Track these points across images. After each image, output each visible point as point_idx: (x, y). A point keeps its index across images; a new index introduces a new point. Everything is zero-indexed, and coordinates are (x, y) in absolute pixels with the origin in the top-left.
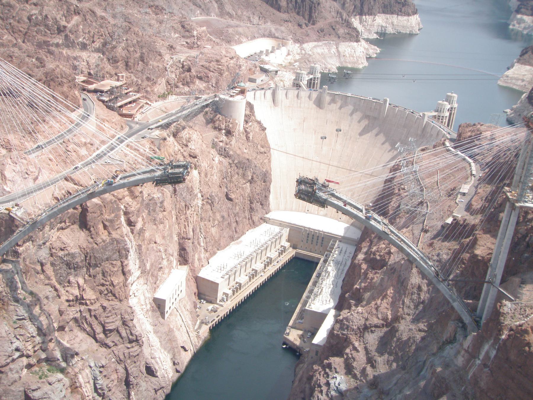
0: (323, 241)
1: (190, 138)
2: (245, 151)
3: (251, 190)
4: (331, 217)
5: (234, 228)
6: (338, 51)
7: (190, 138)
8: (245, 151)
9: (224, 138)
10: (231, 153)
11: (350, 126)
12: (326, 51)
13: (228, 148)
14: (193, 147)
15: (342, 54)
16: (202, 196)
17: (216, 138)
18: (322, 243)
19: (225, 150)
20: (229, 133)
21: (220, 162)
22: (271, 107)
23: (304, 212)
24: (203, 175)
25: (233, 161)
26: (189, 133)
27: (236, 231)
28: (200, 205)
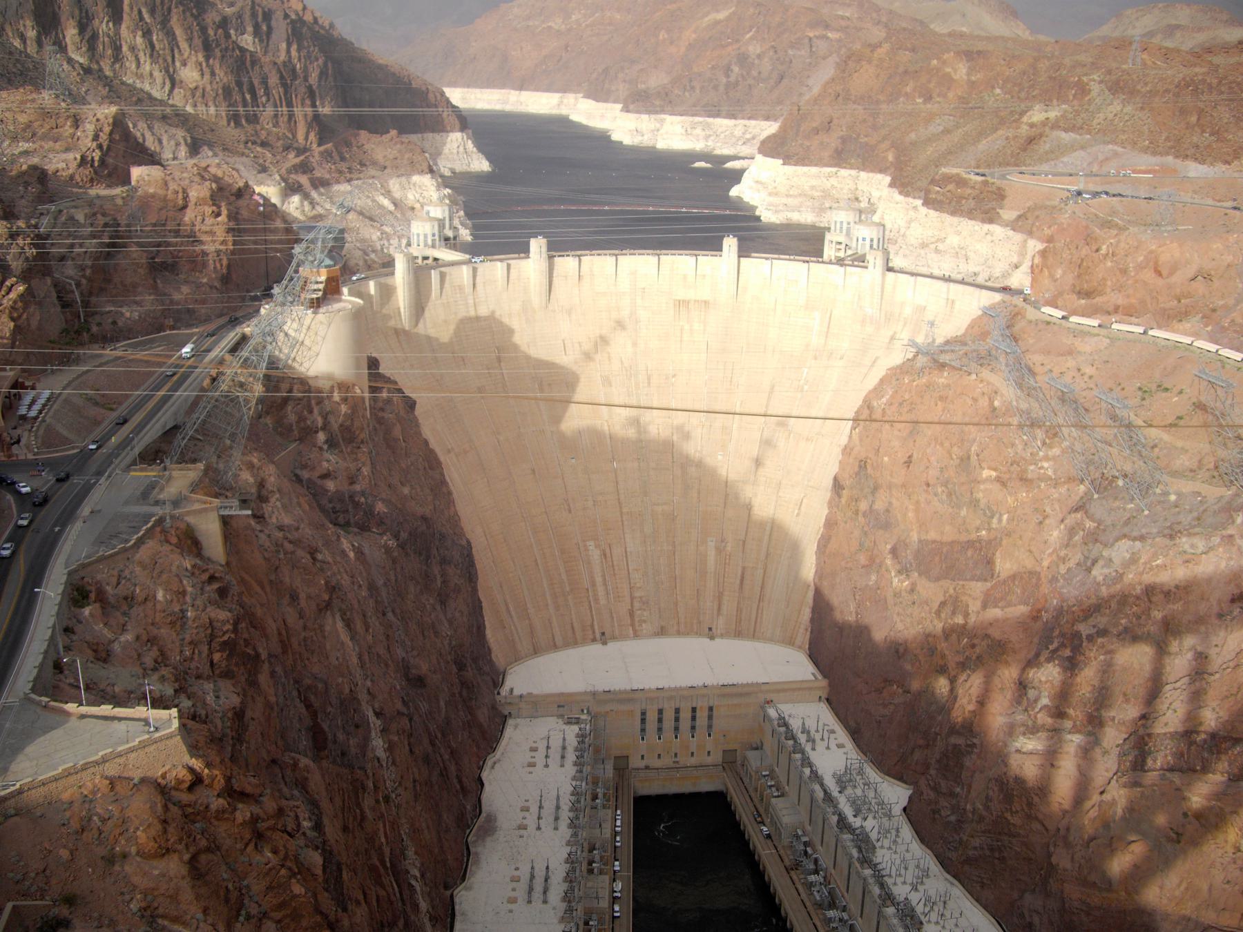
0: (710, 717)
1: (261, 484)
2: (406, 491)
3: (450, 622)
5: (455, 781)
7: (261, 484)
8: (406, 491)
10: (380, 507)
11: (635, 344)
13: (363, 493)
14: (287, 520)
16: (378, 714)
17: (304, 467)
18: (710, 727)
19: (357, 505)
21: (359, 552)
23: (594, 640)
24: (359, 626)
25: (396, 537)
26: (251, 466)
27: (462, 788)
28: (381, 753)
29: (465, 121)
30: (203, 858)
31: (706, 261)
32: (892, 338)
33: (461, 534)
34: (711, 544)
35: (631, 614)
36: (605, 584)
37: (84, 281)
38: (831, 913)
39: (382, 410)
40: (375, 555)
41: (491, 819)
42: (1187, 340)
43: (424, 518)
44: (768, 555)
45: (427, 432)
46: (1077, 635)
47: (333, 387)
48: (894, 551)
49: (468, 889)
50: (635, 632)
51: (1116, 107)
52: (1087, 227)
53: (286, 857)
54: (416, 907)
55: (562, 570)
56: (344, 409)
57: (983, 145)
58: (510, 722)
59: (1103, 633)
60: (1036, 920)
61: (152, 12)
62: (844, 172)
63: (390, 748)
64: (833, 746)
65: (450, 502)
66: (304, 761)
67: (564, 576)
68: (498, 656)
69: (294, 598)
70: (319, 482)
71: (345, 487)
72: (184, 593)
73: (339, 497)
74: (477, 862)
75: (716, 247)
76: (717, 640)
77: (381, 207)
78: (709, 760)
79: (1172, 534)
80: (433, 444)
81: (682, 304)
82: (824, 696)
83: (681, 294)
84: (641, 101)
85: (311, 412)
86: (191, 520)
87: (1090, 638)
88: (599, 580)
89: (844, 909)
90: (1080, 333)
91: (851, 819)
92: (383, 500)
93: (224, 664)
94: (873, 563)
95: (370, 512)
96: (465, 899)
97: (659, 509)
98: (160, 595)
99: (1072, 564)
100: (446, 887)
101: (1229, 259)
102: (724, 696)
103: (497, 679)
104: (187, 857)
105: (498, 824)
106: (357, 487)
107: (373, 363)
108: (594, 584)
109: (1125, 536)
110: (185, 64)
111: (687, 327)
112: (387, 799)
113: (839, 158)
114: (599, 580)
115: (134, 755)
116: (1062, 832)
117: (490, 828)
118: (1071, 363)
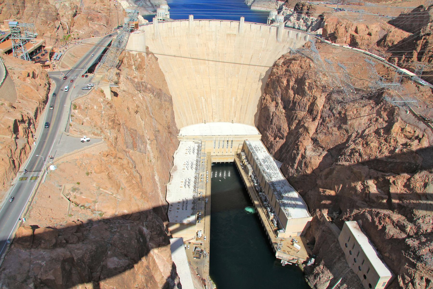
0: (232, 143)
2: (156, 82)
3: (166, 117)
4: (224, 121)
6: (151, 3)
9: (136, 73)
10: (149, 86)
11: (216, 45)
12: (144, 3)
13: (144, 82)
15: (154, 5)
17: (129, 75)
19: (143, 85)
20: (139, 68)
21: (143, 97)
22: (153, 40)
23: (202, 122)
25: (153, 94)
30: (110, 174)
31: (235, 24)
32: (284, 46)
33: (169, 94)
34: (234, 99)
35: (212, 116)
36: (206, 108)
37: (69, 23)
38: (260, 193)
39: (149, 60)
40: (147, 98)
41: (176, 167)
42: (363, 51)
43: (160, 89)
45: (161, 67)
47: (136, 54)
49: (170, 184)
50: (213, 121)
52: (338, 19)
53: (131, 174)
54: (158, 188)
55: (195, 104)
56: (139, 60)
58: (181, 142)
60: (312, 197)
63: (152, 148)
64: (263, 152)
65: (167, 86)
66: (131, 151)
67: (195, 106)
68: (178, 126)
69: (128, 109)
70: (133, 79)
71: (140, 81)
72: (101, 107)
73: (138, 83)
74: (172, 178)
75: (238, 19)
76: (234, 124)
77: (147, 5)
78: (231, 154)
80: (162, 70)
81: (229, 35)
82: (260, 138)
83: (228, 32)
85: (131, 60)
86: (103, 88)
88: (204, 107)
89: (264, 192)
90: (335, 47)
91: (266, 170)
92: (150, 84)
93: (112, 125)
95: (146, 88)
96: (170, 187)
97: (220, 89)
98: (95, 107)
100: (165, 184)
101: (376, 29)
102: (235, 137)
103: (178, 131)
104: (107, 173)
105: (178, 168)
106: (143, 81)
107: (147, 48)
108: (203, 108)
111: (230, 41)
112: (151, 161)
114: (204, 107)
115: (93, 148)
116: (320, 176)
117: (175, 170)
118: (331, 56)
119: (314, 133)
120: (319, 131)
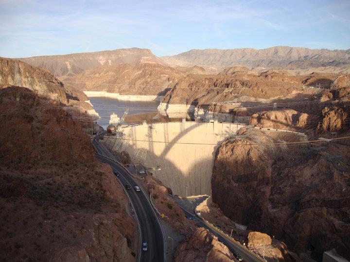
29: (88, 99)
44: (200, 184)
46: (280, 188)
48: (232, 179)
51: (244, 88)
57: (216, 98)
59: (286, 186)
61: (29, 73)
62: (182, 105)
79: (296, 165)
84: (121, 92)
87: (283, 188)
94: (229, 182)
99: (275, 175)
109: (286, 167)
110: (36, 85)
113: (181, 102)
119: (271, 195)
120: (274, 193)
